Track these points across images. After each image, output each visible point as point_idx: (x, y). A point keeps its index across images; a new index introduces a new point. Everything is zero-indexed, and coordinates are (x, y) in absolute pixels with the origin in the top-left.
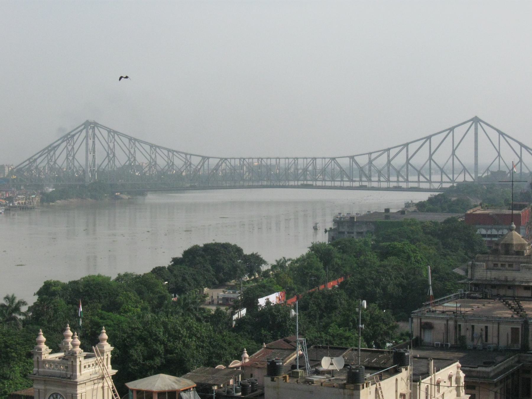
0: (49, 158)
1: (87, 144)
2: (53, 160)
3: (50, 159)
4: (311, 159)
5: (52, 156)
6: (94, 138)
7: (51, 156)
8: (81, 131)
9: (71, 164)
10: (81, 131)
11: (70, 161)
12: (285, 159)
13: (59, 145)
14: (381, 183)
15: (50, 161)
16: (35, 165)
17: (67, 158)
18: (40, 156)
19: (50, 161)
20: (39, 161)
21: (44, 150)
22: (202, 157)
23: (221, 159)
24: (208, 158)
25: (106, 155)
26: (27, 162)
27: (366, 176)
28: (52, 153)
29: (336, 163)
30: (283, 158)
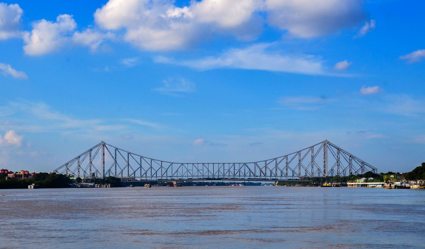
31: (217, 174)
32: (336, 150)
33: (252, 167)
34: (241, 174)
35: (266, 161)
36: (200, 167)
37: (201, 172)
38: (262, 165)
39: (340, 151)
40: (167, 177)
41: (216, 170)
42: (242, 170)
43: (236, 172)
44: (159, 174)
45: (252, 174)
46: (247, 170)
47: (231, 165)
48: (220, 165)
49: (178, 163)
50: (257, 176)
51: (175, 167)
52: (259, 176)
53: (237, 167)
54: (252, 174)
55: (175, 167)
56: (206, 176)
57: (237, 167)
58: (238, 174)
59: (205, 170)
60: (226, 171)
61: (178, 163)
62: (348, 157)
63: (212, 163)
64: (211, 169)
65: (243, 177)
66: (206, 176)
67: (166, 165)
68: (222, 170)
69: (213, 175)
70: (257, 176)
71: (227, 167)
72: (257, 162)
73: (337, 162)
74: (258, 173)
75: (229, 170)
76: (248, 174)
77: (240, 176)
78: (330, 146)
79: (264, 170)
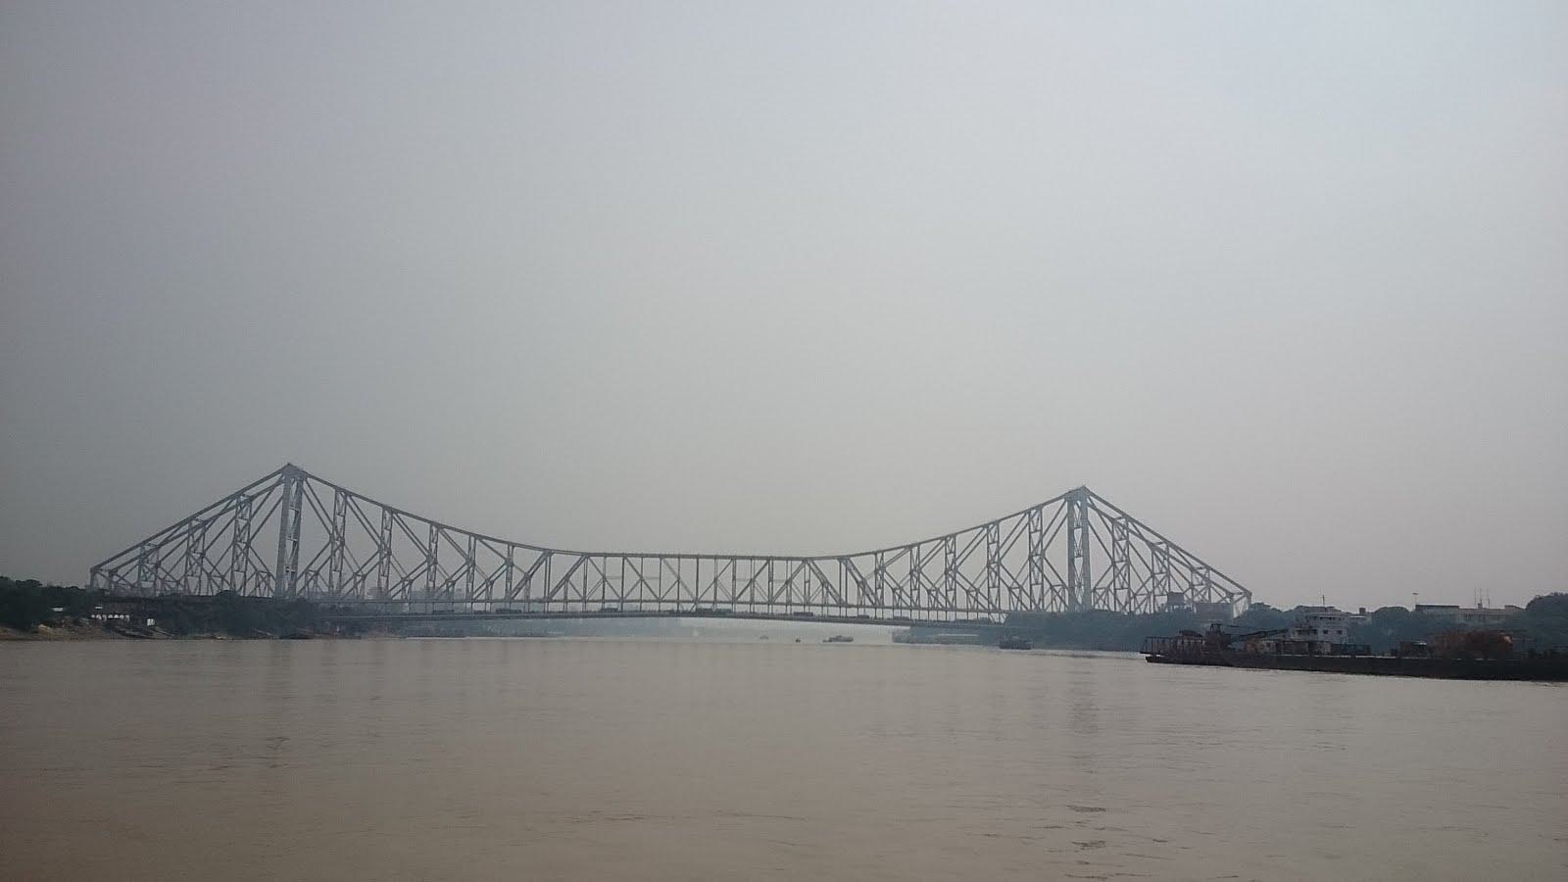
0: (191, 544)
1: (285, 515)
2: (200, 550)
3: (193, 546)
5: (198, 540)
6: (299, 504)
7: (195, 538)
8: (271, 489)
9: (240, 558)
10: (271, 489)
11: (239, 551)
13: (216, 517)
14: (885, 610)
15: (192, 549)
16: (154, 560)
17: (235, 543)
18: (166, 541)
19: (192, 549)
20: (164, 550)
21: (181, 524)
22: (544, 550)
23: (583, 554)
24: (548, 553)
25: (328, 540)
26: (137, 552)
28: (198, 534)
33: (830, 570)
36: (651, 567)
37: (653, 584)
41: (706, 579)
42: (798, 581)
43: (777, 587)
44: (499, 592)
46: (815, 583)
51: (560, 565)
53: (781, 570)
55: (560, 565)
57: (781, 570)
64: (688, 577)
65: (800, 609)
67: (524, 559)
68: (726, 580)
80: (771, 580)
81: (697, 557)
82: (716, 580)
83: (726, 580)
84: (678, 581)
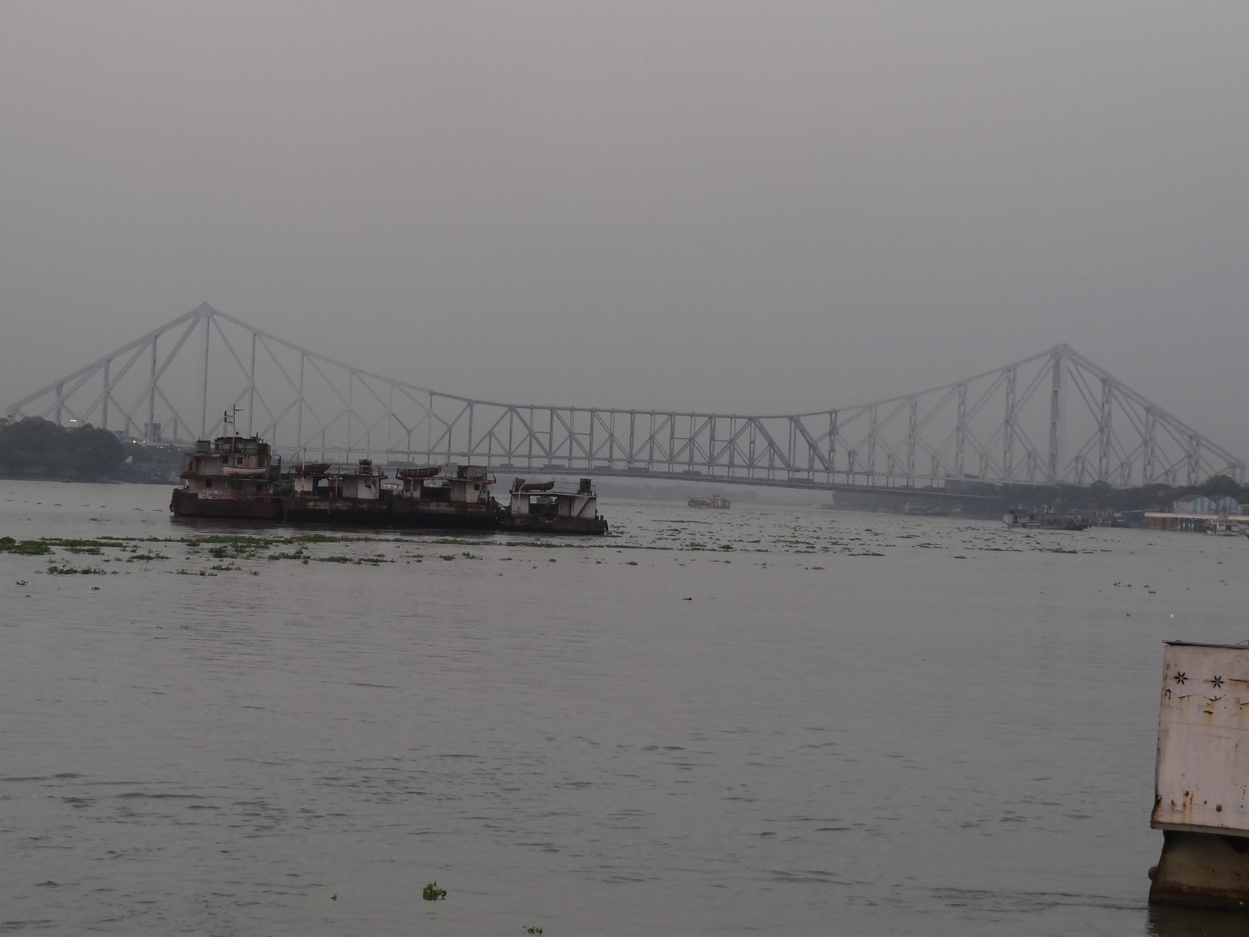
4: (507, 408)
12: (611, 412)
24: (471, 403)
27: (821, 459)
29: (758, 428)
30: (687, 415)
31: (645, 455)
32: (1097, 387)
33: (780, 431)
34: (738, 460)
35: (833, 413)
36: (581, 422)
37: (585, 441)
38: (817, 427)
39: (1116, 392)
40: (449, 454)
41: (641, 437)
42: (743, 442)
45: (778, 463)
46: (762, 444)
47: (701, 421)
48: (660, 419)
49: (497, 405)
50: (798, 470)
52: (805, 470)
54: (778, 463)
56: (602, 459)
57: (724, 430)
58: (725, 459)
59: (601, 436)
60: (678, 445)
61: (497, 405)
62: (1142, 413)
63: (629, 412)
64: (622, 436)
66: (602, 459)
69: (631, 459)
70: (798, 470)
71: (683, 427)
72: (799, 416)
73: (1102, 430)
74: (802, 460)
75: (691, 440)
76: (765, 462)
77: (731, 464)
78: (1080, 368)
79: (824, 447)
80: (712, 438)
81: (632, 413)
82: (652, 438)
83: (663, 438)
84: (611, 435)
